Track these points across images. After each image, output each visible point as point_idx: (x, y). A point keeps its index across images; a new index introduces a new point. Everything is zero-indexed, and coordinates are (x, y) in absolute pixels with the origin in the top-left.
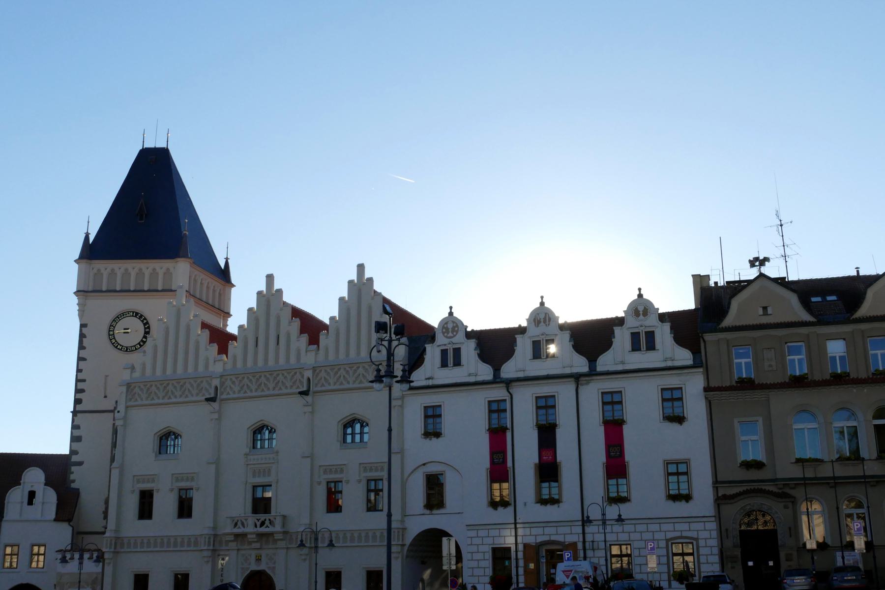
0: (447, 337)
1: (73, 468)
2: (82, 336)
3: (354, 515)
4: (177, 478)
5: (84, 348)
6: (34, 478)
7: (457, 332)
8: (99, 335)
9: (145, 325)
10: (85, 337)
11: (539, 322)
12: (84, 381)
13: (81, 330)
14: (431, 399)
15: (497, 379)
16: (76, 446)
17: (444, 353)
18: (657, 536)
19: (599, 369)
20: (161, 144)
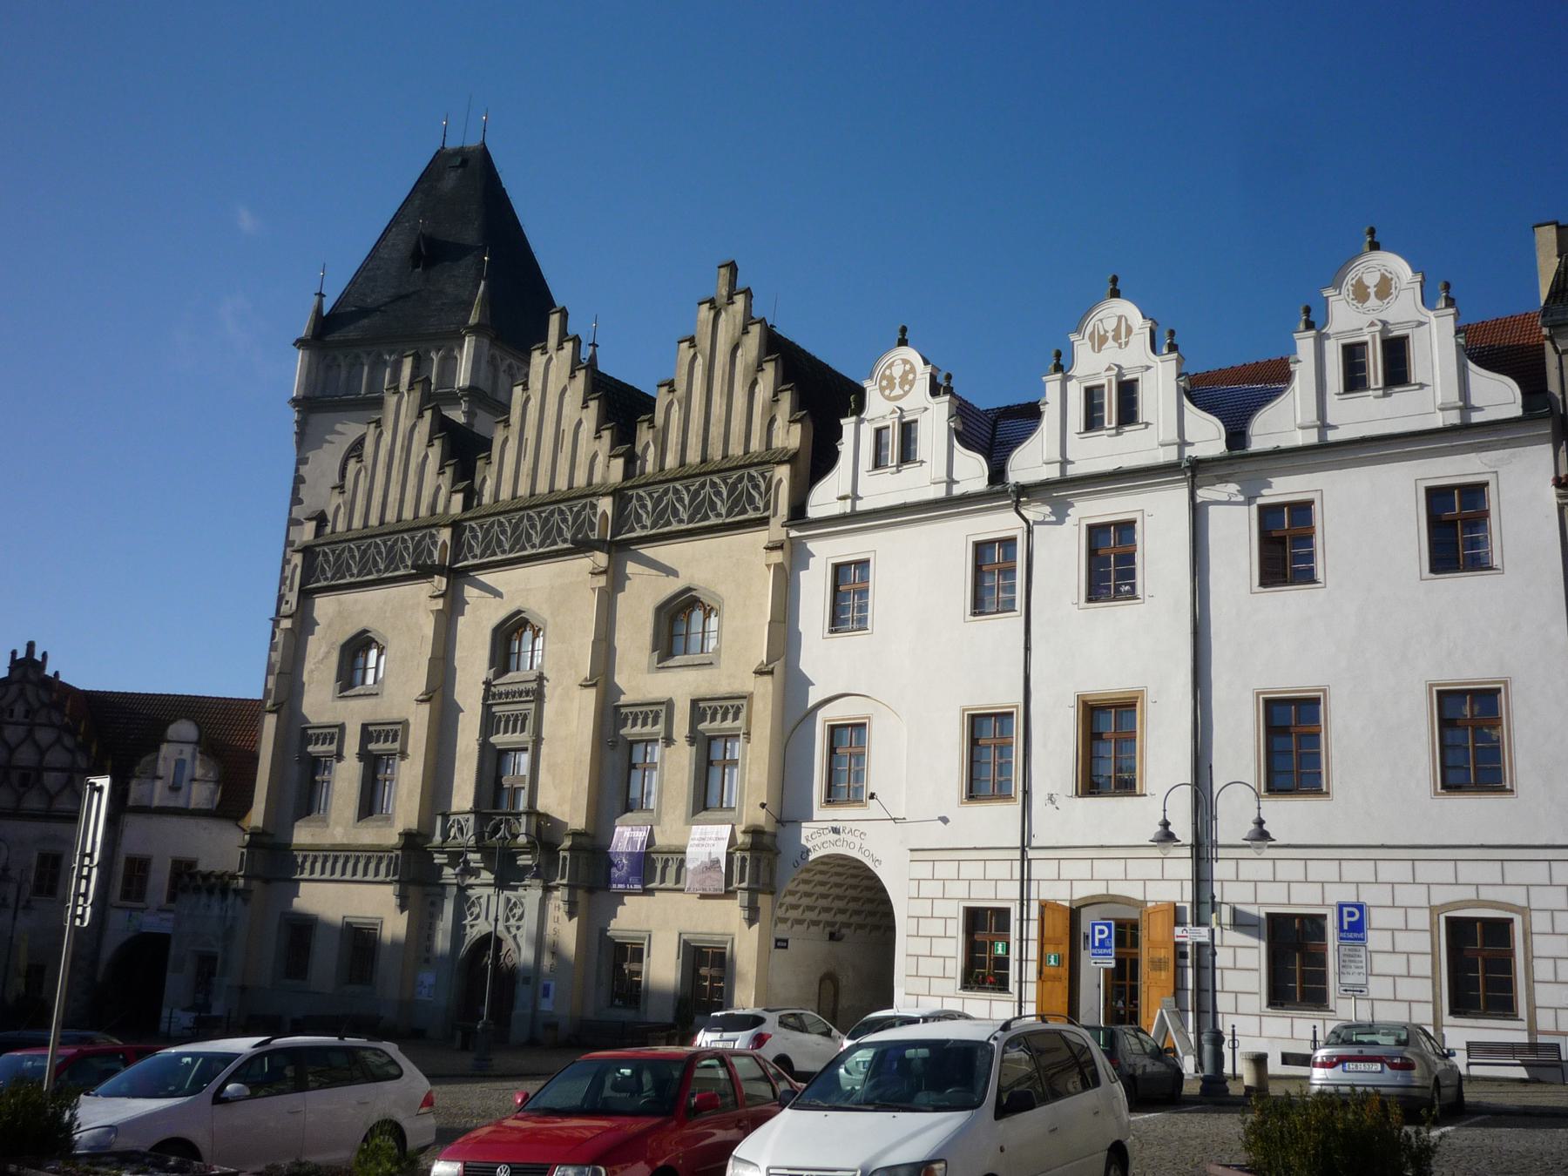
0: (888, 398)
2: (299, 480)
5: (300, 502)
6: (184, 729)
7: (912, 384)
10: (303, 481)
11: (1103, 340)
13: (297, 470)
14: (846, 547)
15: (999, 488)
18: (1406, 895)
19: (1257, 444)
20: (472, 142)
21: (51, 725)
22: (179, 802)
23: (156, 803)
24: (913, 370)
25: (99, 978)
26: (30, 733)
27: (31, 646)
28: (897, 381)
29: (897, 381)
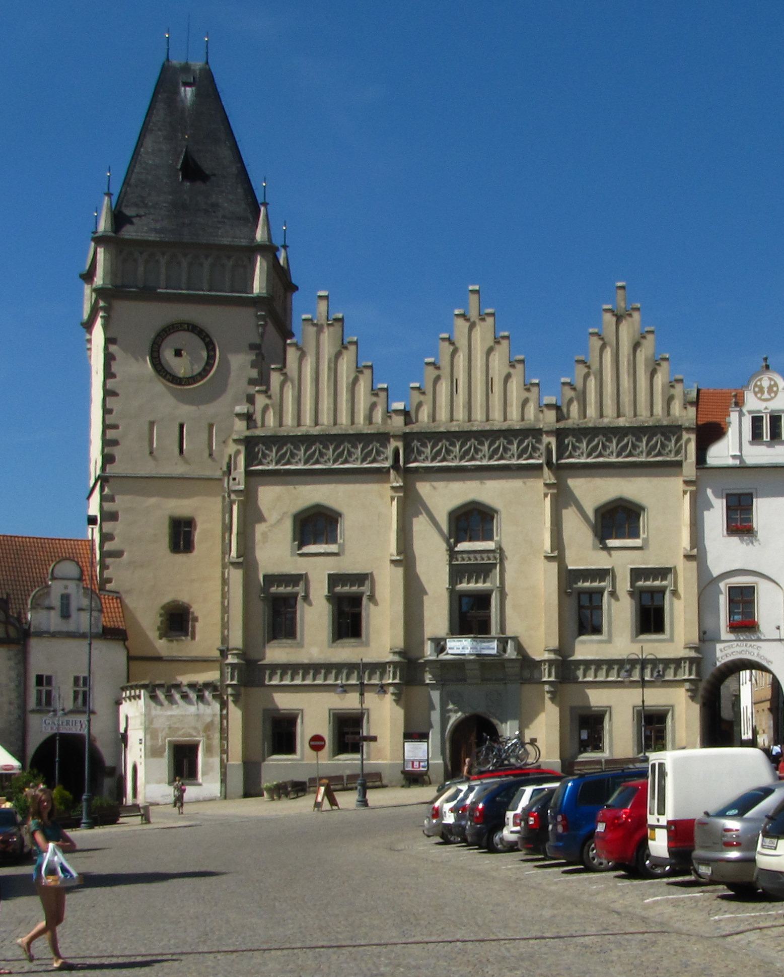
3: (618, 638)
4: (334, 580)
5: (113, 376)
13: (106, 348)
17: (757, 422)
22: (71, 626)
23: (52, 629)
24: (776, 385)
28: (766, 390)
29: (766, 390)
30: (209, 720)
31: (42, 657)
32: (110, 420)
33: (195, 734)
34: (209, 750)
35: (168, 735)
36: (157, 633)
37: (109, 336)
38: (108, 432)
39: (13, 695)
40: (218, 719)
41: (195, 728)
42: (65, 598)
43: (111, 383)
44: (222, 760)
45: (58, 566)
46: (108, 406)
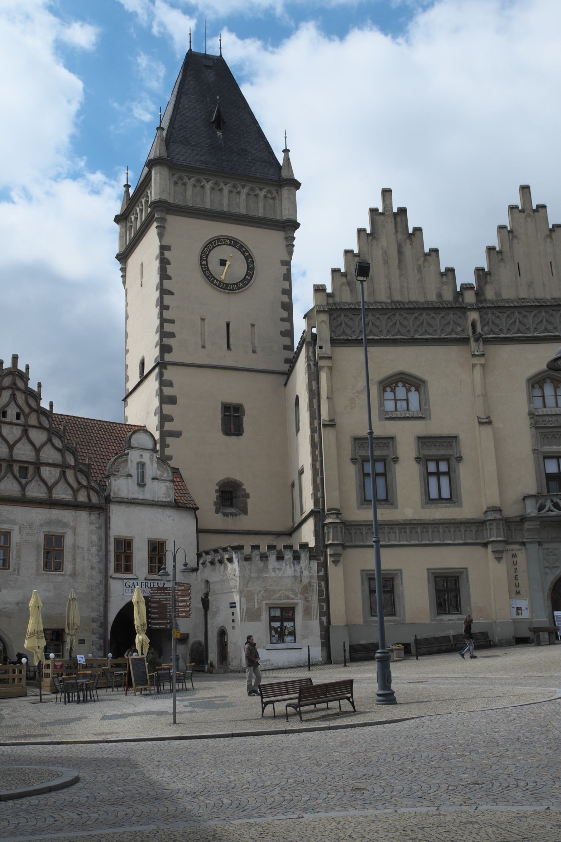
1: (169, 440)
5: (169, 278)
8: (186, 261)
9: (246, 258)
10: (169, 263)
12: (172, 321)
16: (168, 409)
21: (41, 427)
22: (147, 495)
25: (109, 638)
26: (25, 432)
27: (15, 358)
30: (305, 581)
31: (121, 522)
32: (167, 315)
33: (292, 596)
34: (307, 612)
35: (264, 598)
36: (214, 508)
37: (164, 243)
38: (165, 325)
39: (95, 560)
40: (315, 582)
41: (293, 591)
42: (141, 465)
43: (167, 284)
44: (321, 623)
45: (134, 436)
46: (165, 303)
